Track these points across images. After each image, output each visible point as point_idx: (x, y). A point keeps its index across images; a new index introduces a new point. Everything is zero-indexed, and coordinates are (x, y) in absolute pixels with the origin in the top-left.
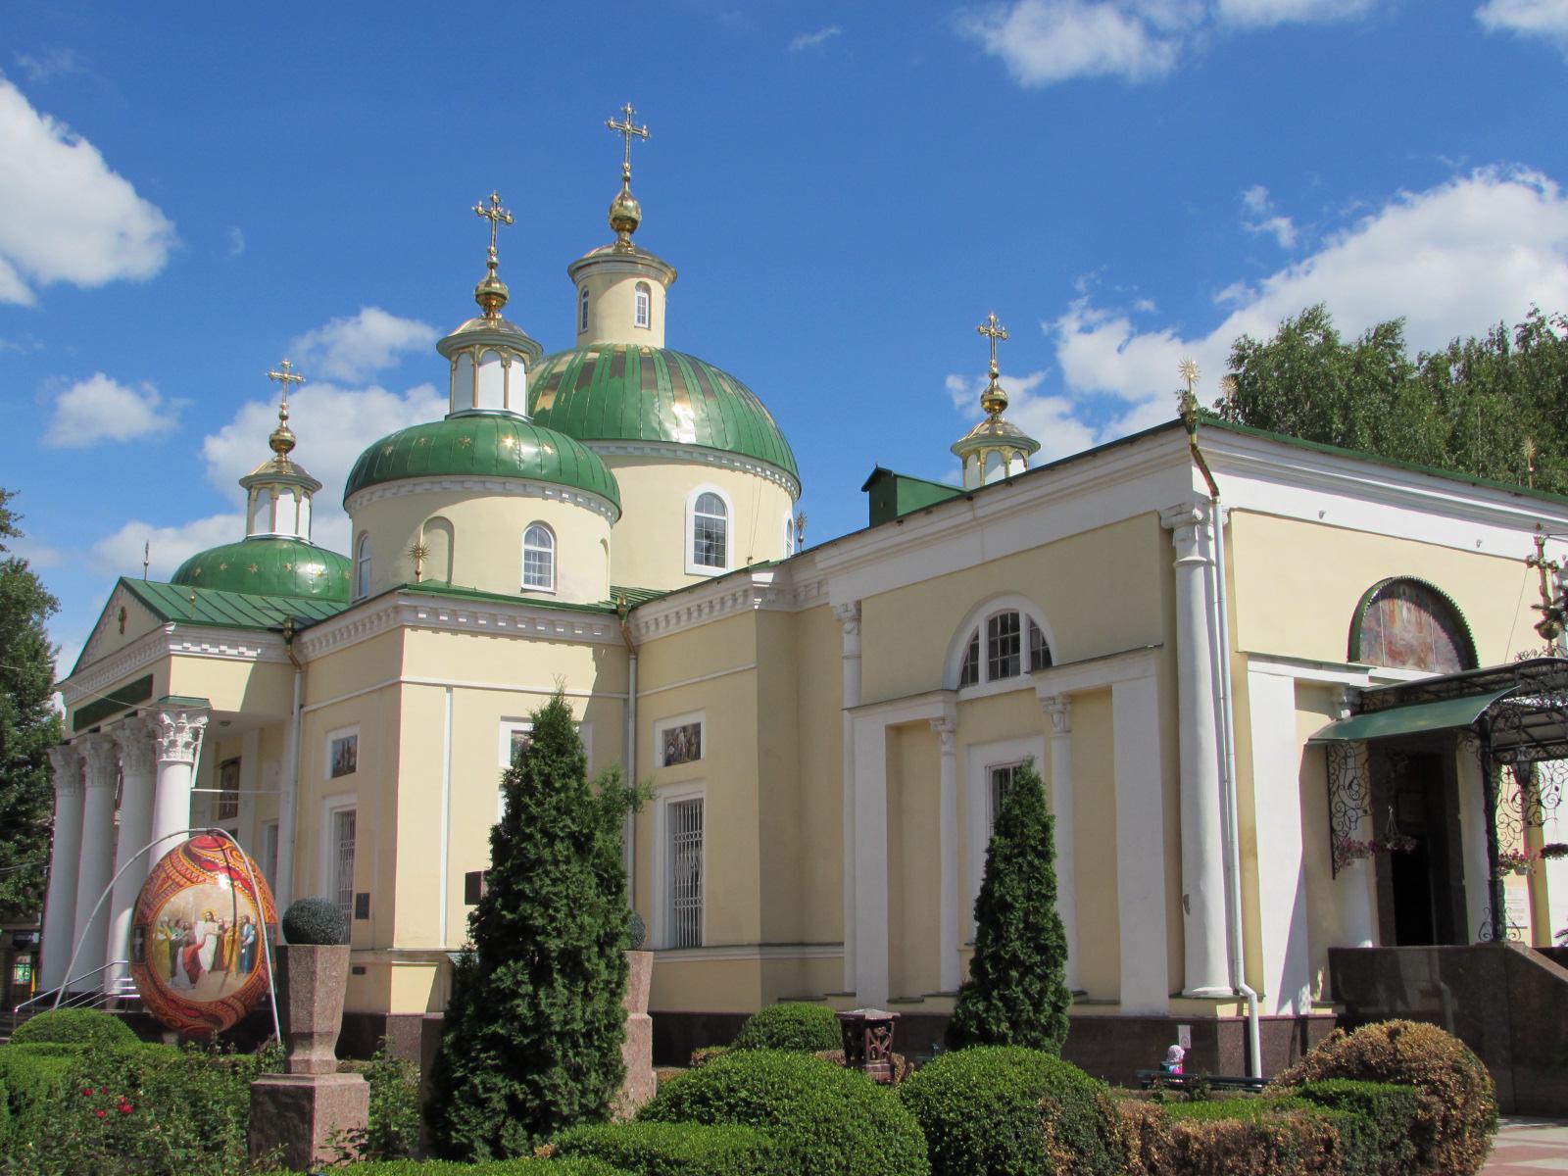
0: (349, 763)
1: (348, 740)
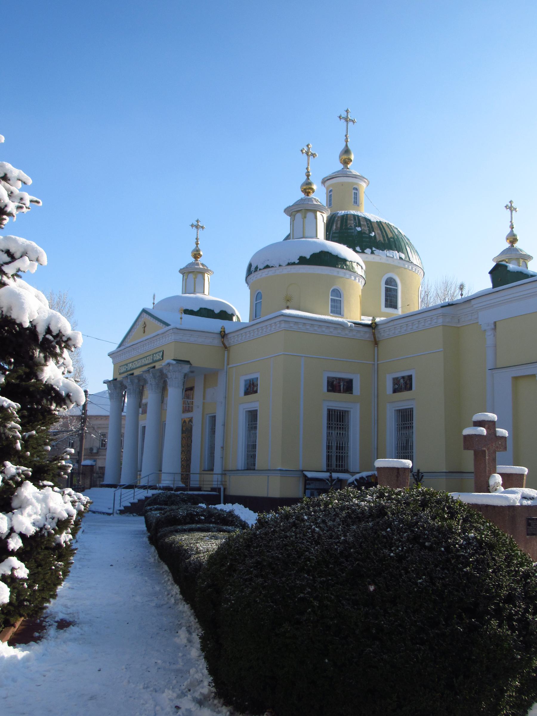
0: (253, 388)
1: (253, 379)
